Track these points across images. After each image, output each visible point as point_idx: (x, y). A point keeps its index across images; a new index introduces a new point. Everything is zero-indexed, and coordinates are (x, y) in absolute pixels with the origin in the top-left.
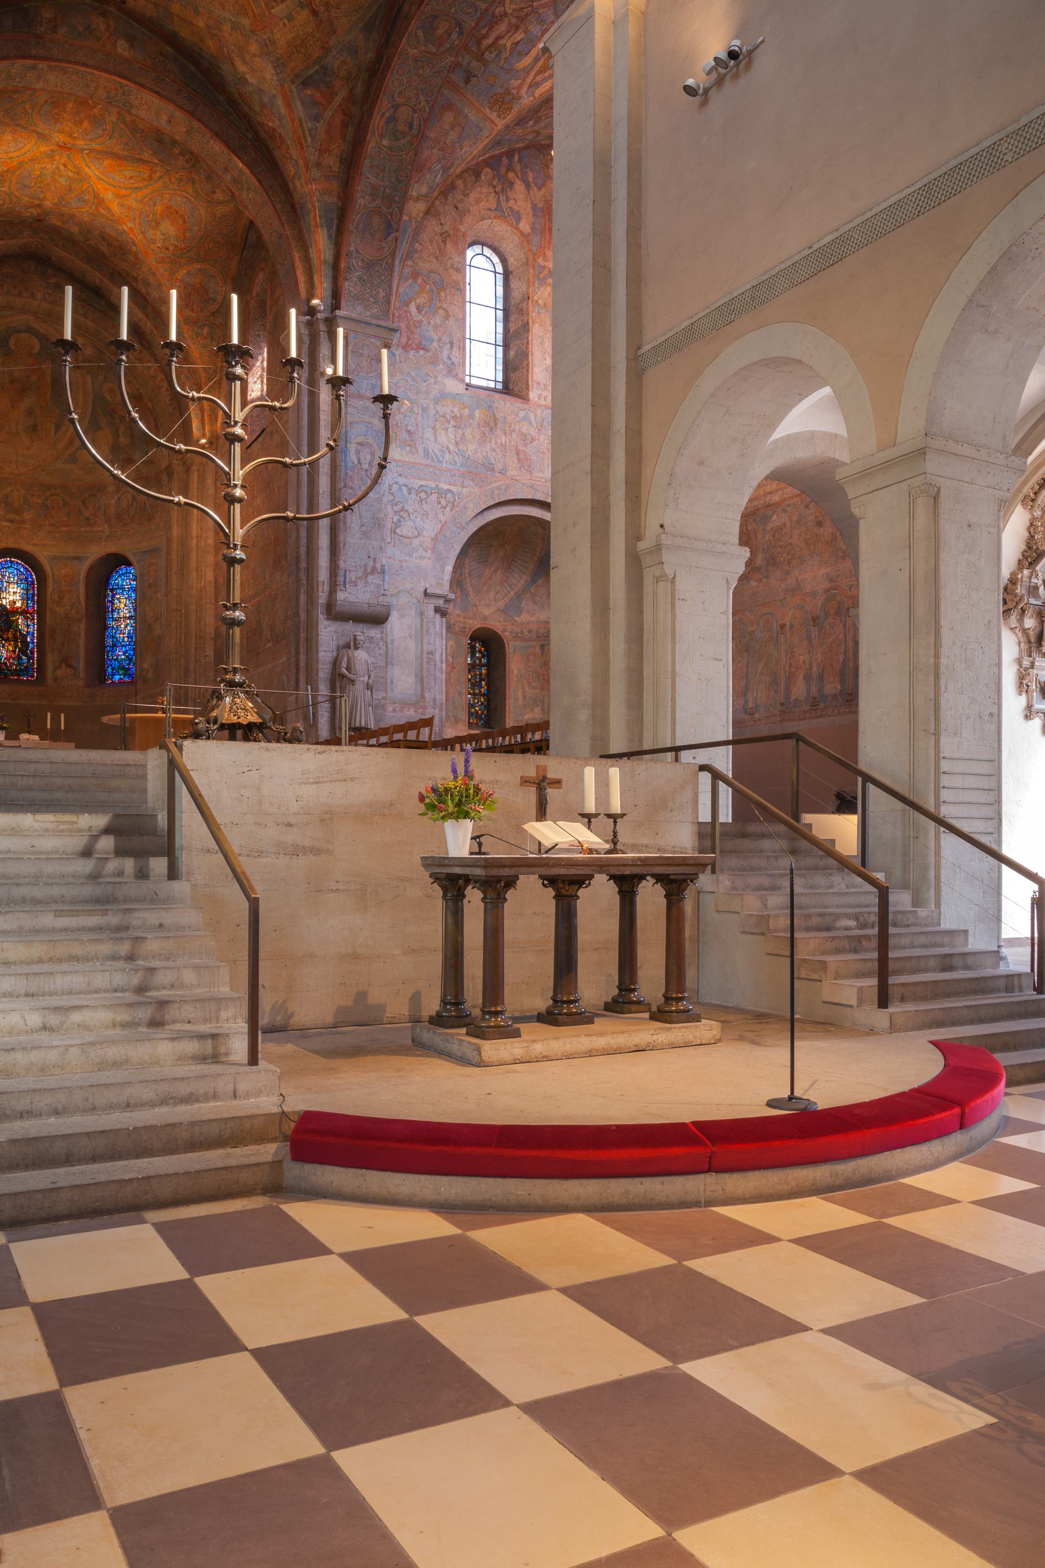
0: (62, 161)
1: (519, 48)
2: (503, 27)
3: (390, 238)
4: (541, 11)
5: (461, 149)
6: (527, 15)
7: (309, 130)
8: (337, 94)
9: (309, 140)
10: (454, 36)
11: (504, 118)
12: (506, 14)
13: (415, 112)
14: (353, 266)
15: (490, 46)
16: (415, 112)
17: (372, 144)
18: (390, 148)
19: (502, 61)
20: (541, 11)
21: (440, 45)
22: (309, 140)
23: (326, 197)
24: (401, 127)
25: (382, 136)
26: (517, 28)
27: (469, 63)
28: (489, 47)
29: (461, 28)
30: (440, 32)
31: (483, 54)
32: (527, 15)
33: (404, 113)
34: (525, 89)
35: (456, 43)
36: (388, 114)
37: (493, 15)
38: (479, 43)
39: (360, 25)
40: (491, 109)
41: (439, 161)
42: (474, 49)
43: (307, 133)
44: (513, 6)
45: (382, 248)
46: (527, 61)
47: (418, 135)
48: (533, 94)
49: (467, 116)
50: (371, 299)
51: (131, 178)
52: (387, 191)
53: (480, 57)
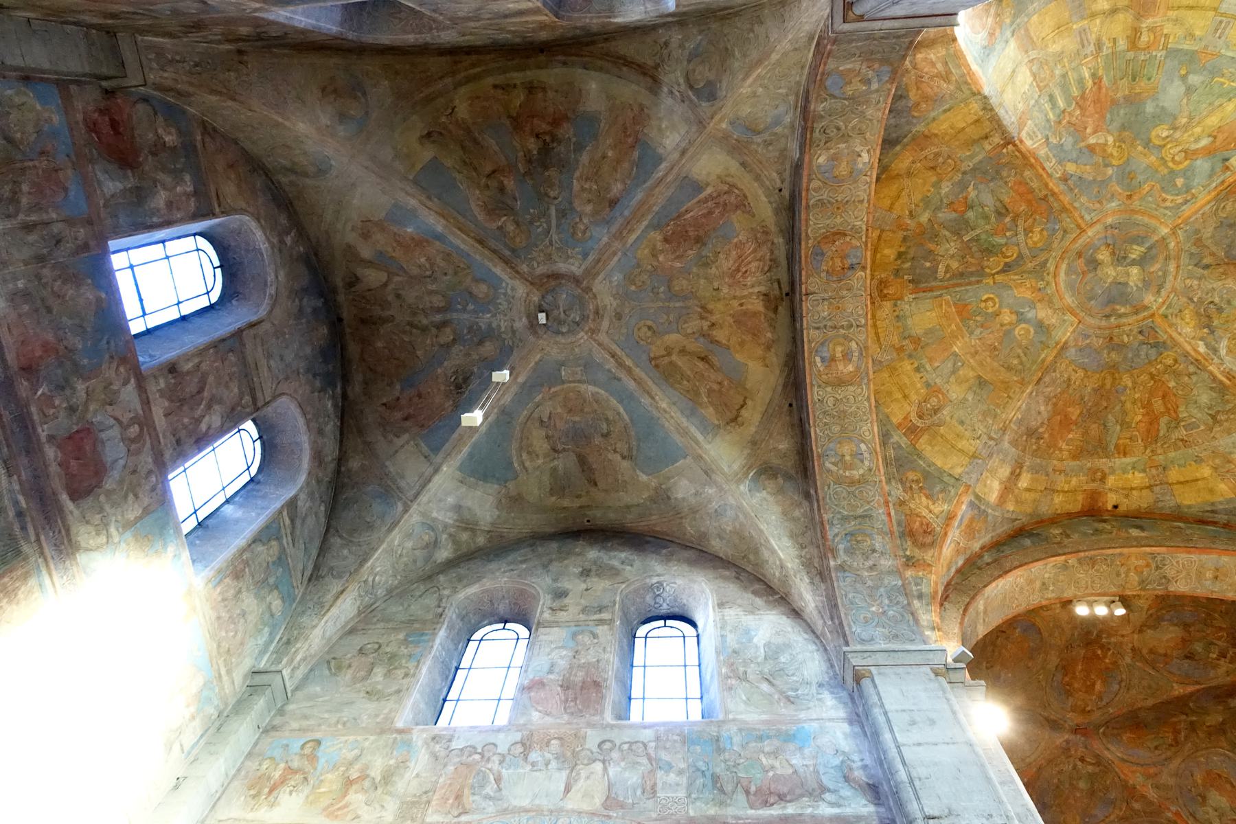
0: (1079, 754)
51: (1156, 748)
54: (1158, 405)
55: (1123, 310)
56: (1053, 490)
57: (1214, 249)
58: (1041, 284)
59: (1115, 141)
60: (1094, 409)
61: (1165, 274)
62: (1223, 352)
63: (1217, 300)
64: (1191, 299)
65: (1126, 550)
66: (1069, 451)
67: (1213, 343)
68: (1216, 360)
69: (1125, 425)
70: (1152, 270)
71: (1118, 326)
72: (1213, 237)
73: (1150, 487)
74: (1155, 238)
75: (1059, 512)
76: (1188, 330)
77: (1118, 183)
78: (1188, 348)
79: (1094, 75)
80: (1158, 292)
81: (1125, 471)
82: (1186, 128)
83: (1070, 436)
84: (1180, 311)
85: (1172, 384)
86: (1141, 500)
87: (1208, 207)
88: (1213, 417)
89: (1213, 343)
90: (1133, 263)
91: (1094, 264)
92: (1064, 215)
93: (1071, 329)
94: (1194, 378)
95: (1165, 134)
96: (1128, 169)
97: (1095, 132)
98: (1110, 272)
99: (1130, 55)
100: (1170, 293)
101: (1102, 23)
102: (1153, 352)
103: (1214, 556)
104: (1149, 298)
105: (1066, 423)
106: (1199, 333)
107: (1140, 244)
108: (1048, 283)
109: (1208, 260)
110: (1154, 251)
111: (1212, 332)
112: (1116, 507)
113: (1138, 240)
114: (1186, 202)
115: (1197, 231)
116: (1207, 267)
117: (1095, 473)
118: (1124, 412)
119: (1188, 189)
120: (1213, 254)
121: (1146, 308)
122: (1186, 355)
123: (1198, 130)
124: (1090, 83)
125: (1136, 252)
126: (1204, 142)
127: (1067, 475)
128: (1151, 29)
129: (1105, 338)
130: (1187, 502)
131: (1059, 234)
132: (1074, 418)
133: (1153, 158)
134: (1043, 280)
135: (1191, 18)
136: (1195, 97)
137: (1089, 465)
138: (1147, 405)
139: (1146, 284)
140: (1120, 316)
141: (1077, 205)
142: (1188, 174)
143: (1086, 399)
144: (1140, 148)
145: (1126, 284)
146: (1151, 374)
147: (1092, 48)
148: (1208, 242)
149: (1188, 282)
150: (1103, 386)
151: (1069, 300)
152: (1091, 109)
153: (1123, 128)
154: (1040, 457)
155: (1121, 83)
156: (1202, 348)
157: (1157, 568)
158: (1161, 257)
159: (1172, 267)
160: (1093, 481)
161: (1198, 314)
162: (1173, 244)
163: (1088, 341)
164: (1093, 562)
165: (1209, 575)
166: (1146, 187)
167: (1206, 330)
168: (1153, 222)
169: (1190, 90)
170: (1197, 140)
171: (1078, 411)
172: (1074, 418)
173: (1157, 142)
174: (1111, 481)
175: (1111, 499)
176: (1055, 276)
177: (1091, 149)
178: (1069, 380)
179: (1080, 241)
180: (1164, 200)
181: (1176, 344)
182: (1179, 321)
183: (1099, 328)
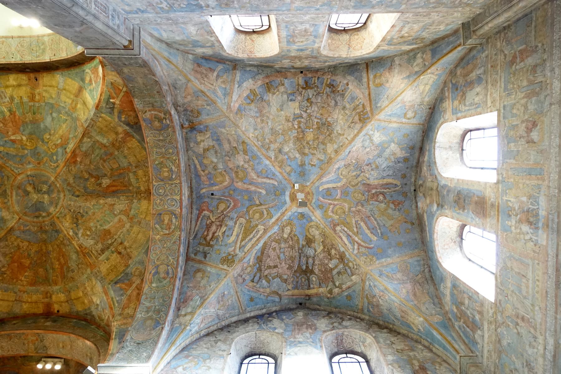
1: (226, 233)
2: (214, 228)
3: (158, 328)
4: (229, 215)
5: (210, 286)
6: (223, 219)
7: (117, 301)
8: (134, 283)
9: (117, 305)
10: (174, 220)
11: (232, 266)
12: (213, 222)
13: (168, 266)
14: (127, 346)
15: (212, 238)
16: (168, 266)
17: (146, 287)
18: (157, 287)
19: (220, 243)
20: (229, 215)
21: (170, 228)
22: (117, 305)
23: (122, 327)
24: (162, 275)
25: (151, 283)
26: (221, 226)
27: (203, 249)
28: (211, 239)
29: (175, 215)
30: (166, 222)
31: (209, 243)
32: (223, 219)
33: (162, 269)
34: (238, 250)
35: (177, 224)
36: (153, 272)
37: (207, 224)
38: (205, 239)
39: (144, 251)
40: (222, 265)
41: (198, 295)
42: (204, 242)
43: (115, 302)
44: (215, 218)
45: (151, 334)
46: (233, 238)
47: (173, 277)
48: (243, 251)
49: (210, 272)
50: (135, 359)
52: (157, 307)
53: (208, 245)
54: (62, 260)
55: (44, 214)
56: (21, 301)
57: (78, 188)
58: (6, 201)
59: (27, 139)
60: (39, 261)
61: (59, 198)
62: (80, 235)
63: (81, 211)
64: (70, 211)
65: (25, 331)
66: (27, 281)
67: (77, 231)
68: (76, 239)
69: (53, 269)
70: (53, 196)
71: (44, 222)
72: (74, 182)
73: (67, 301)
74: (50, 182)
75: (28, 313)
76: (67, 224)
77: (32, 157)
78: (66, 232)
79: (10, 111)
80: (56, 206)
81: (58, 293)
82: (54, 134)
83: (26, 274)
84: (65, 215)
85: (64, 250)
86: (65, 309)
87: (64, 169)
88: (78, 266)
89: (77, 231)
90: (45, 193)
91: (27, 193)
92: (4, 169)
93: (15, 222)
94: (70, 247)
95: (48, 137)
96: (37, 151)
97: (14, 134)
98: (35, 197)
99: (32, 104)
100: (61, 207)
101: (13, 91)
102: (56, 234)
103: (61, 335)
104: (52, 209)
105: (22, 267)
106: (71, 226)
107: (46, 185)
108: (9, 200)
109: (77, 193)
110: (52, 188)
111: (77, 226)
112: (58, 311)
113: (45, 183)
114: (57, 166)
115: (66, 180)
116: (78, 196)
117: (47, 293)
118: (52, 263)
119: (57, 160)
120: (78, 190)
121: (51, 214)
122: (65, 236)
123: (57, 136)
124: (8, 114)
125: (45, 188)
126: (59, 141)
127: (28, 293)
128: (39, 94)
129: (38, 227)
130: (80, 309)
131: (5, 178)
132: (27, 265)
133: (45, 147)
134: (6, 198)
135: (51, 90)
136: (55, 122)
137: (42, 289)
138: (59, 260)
139: (51, 203)
140: (44, 217)
141: (8, 165)
142: (56, 154)
143: (32, 256)
144: (40, 143)
145: (43, 202)
146: (57, 245)
147: (8, 99)
148: (74, 185)
149: (69, 202)
150: (42, 250)
151: (17, 208)
152: (10, 124)
153: (30, 134)
154: (6, 283)
155: (27, 115)
156: (71, 233)
157: (41, 341)
158: (56, 191)
159: (62, 195)
160: (47, 298)
161: (73, 217)
162: (58, 185)
163: (28, 228)
164: (9, 337)
165: (61, 345)
166: (45, 159)
167: (75, 225)
168: (49, 175)
169: (53, 119)
170: (57, 140)
171: (29, 262)
172: (27, 265)
173: (46, 141)
174: (54, 297)
175: (56, 307)
176: (11, 197)
177: (14, 141)
178: (18, 245)
179: (16, 182)
180: (51, 165)
181: (62, 231)
182: (64, 220)
183: (34, 222)
